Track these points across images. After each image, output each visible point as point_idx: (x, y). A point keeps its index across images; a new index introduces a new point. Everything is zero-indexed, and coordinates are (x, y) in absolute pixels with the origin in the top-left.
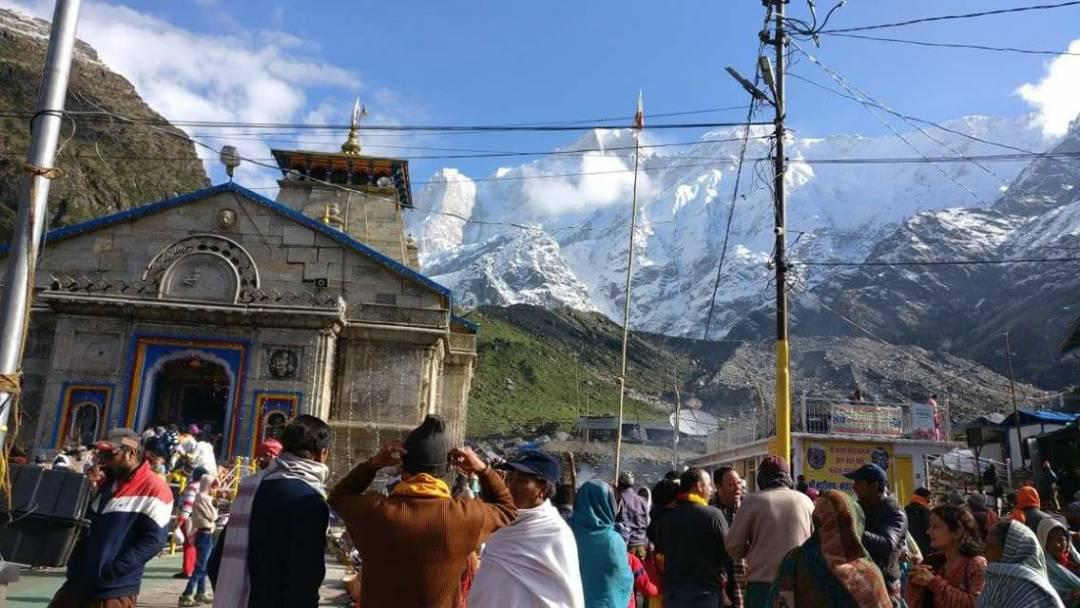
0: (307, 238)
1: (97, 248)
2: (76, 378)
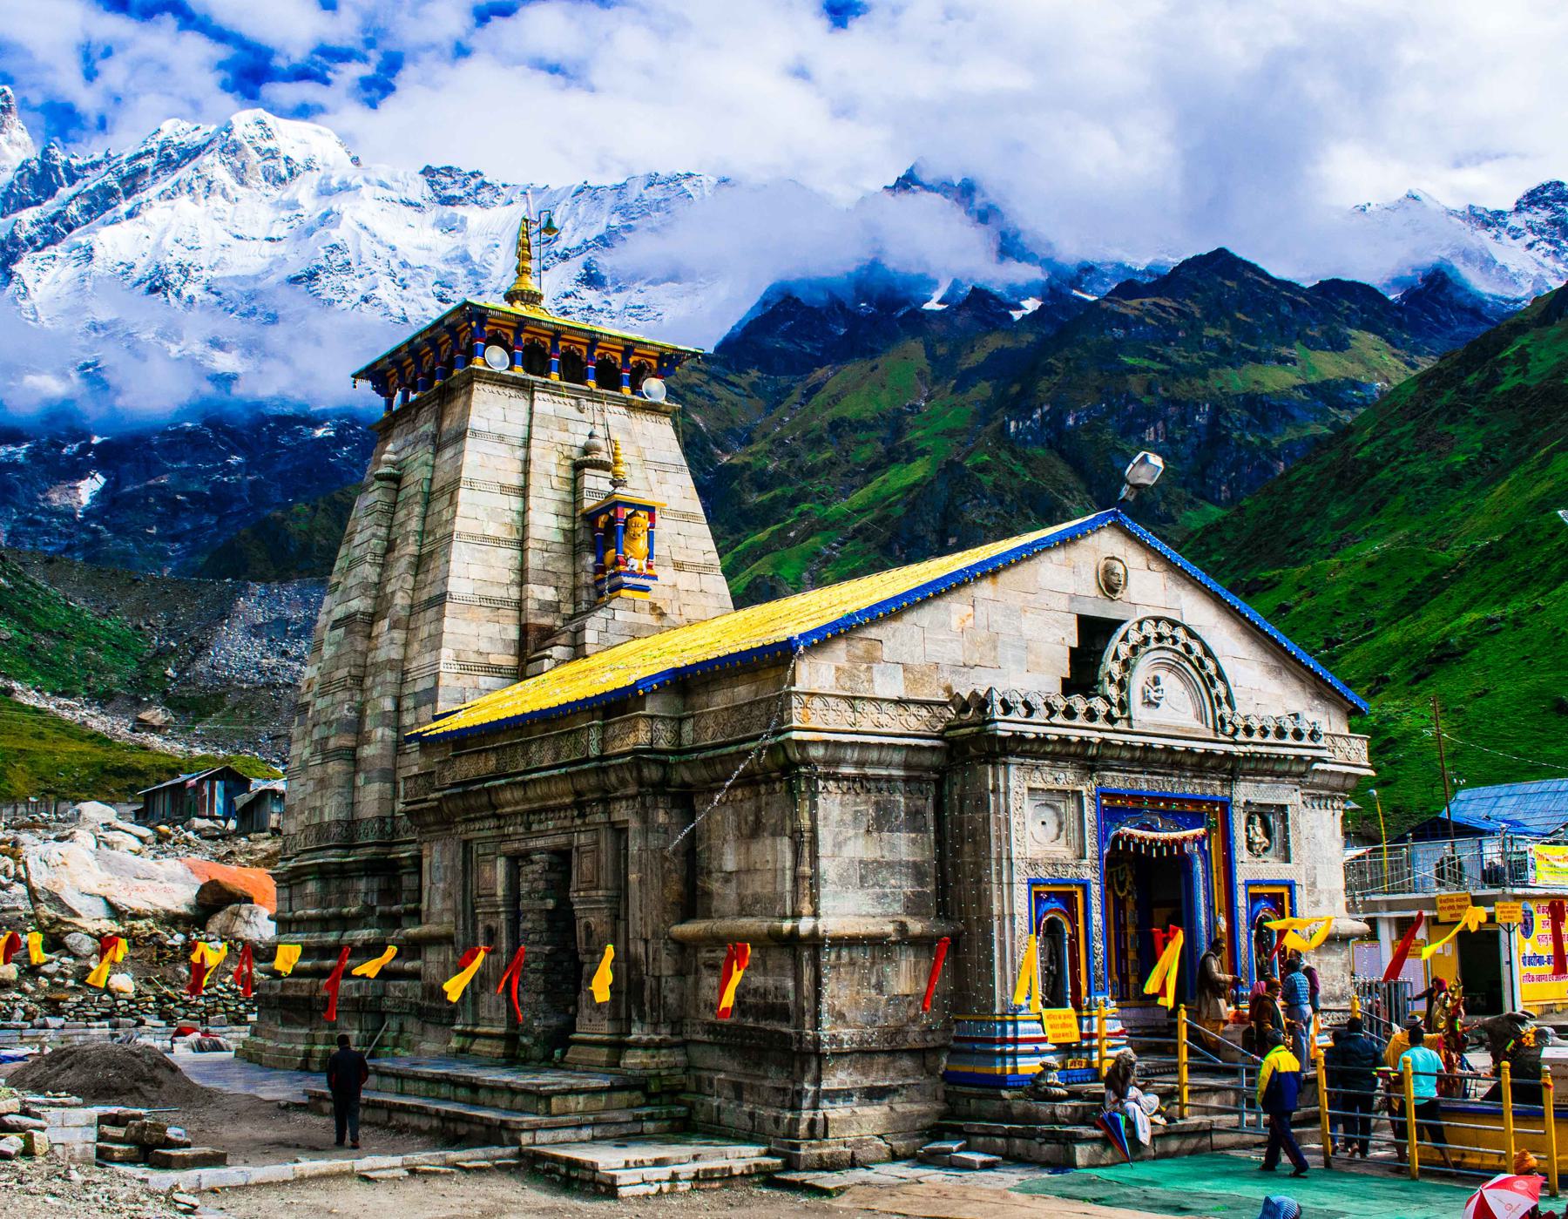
1: (955, 622)
2: (1043, 873)
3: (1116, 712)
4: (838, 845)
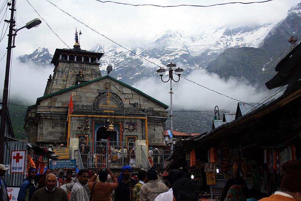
0: (129, 91)
3: (95, 107)
4: (47, 129)
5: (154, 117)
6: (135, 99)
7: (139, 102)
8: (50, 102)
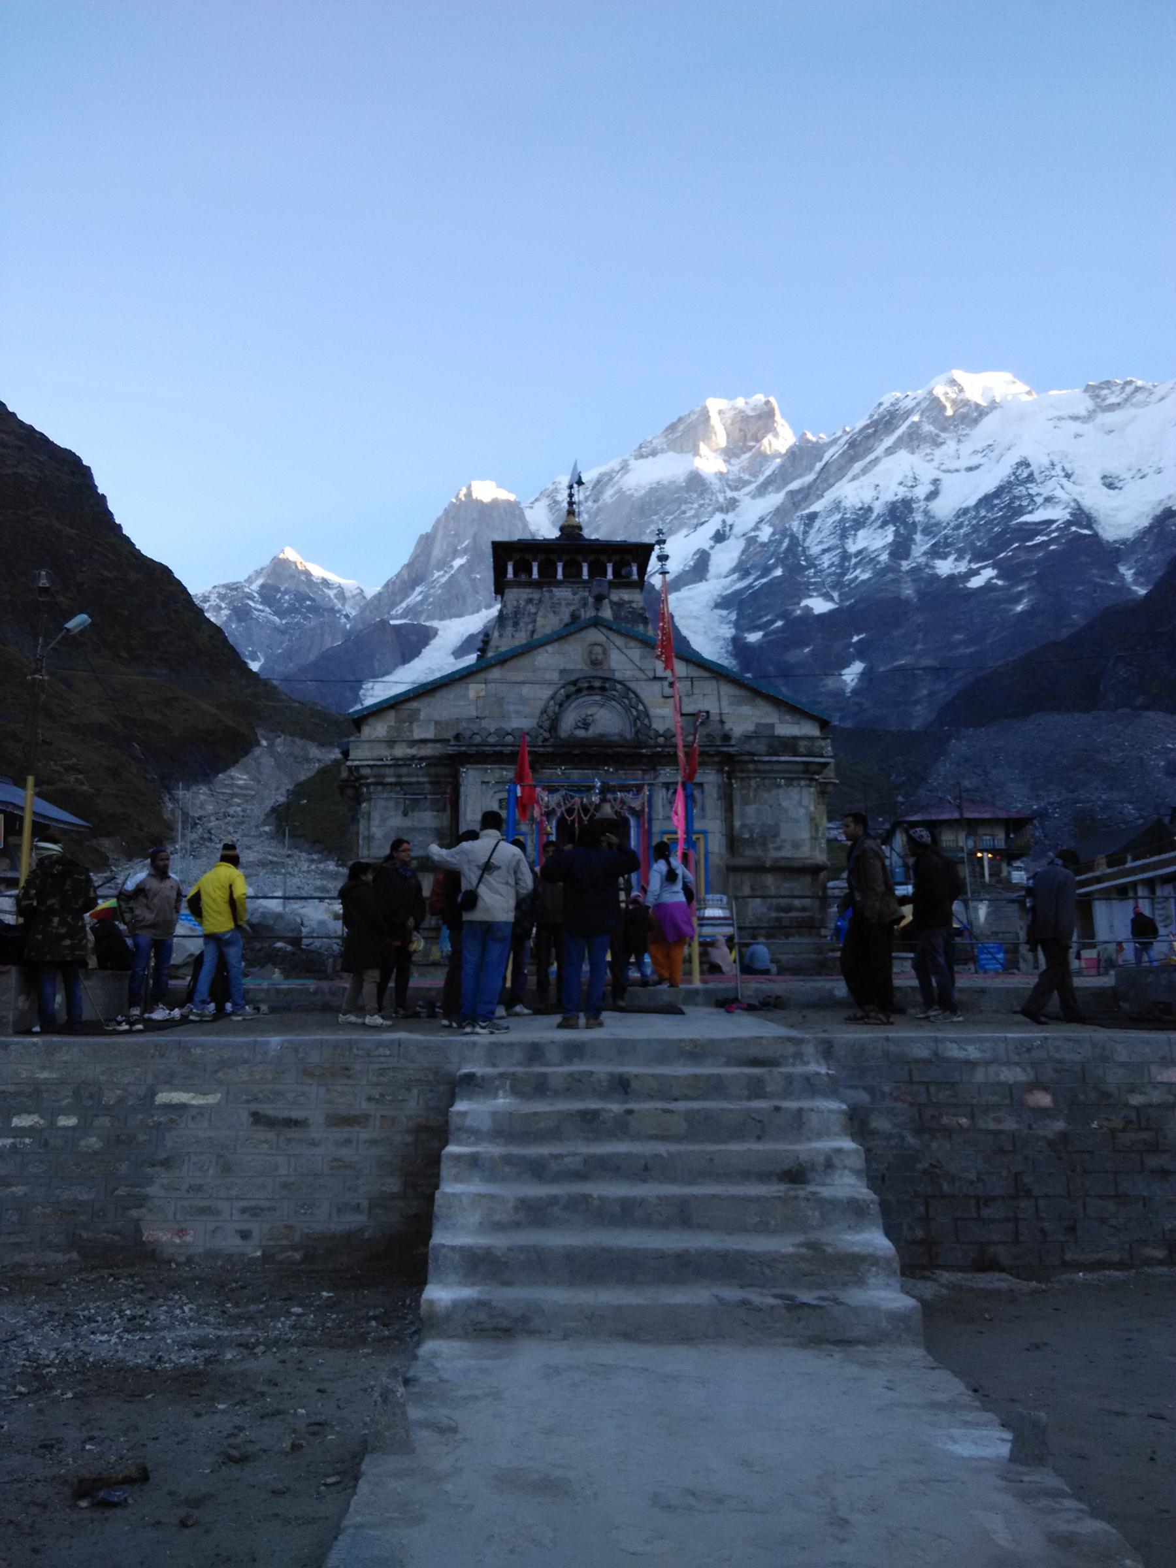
1: (472, 694)
4: (384, 820)
5: (775, 759)
6: (701, 697)
7: (717, 704)
8: (392, 724)
